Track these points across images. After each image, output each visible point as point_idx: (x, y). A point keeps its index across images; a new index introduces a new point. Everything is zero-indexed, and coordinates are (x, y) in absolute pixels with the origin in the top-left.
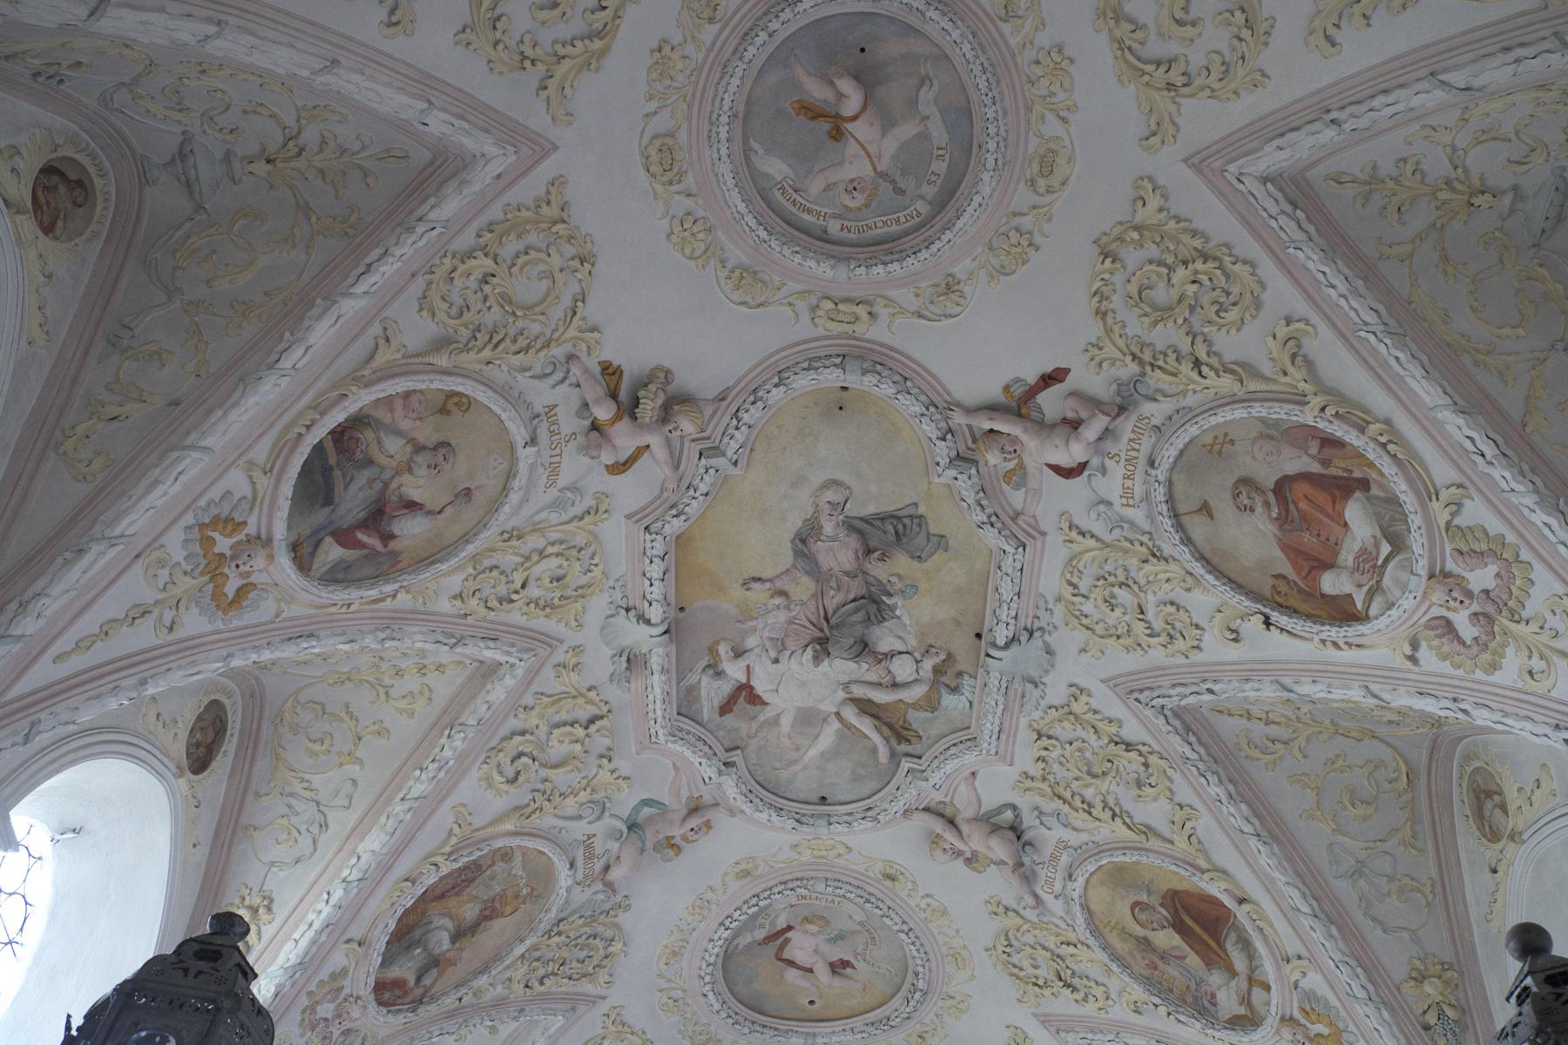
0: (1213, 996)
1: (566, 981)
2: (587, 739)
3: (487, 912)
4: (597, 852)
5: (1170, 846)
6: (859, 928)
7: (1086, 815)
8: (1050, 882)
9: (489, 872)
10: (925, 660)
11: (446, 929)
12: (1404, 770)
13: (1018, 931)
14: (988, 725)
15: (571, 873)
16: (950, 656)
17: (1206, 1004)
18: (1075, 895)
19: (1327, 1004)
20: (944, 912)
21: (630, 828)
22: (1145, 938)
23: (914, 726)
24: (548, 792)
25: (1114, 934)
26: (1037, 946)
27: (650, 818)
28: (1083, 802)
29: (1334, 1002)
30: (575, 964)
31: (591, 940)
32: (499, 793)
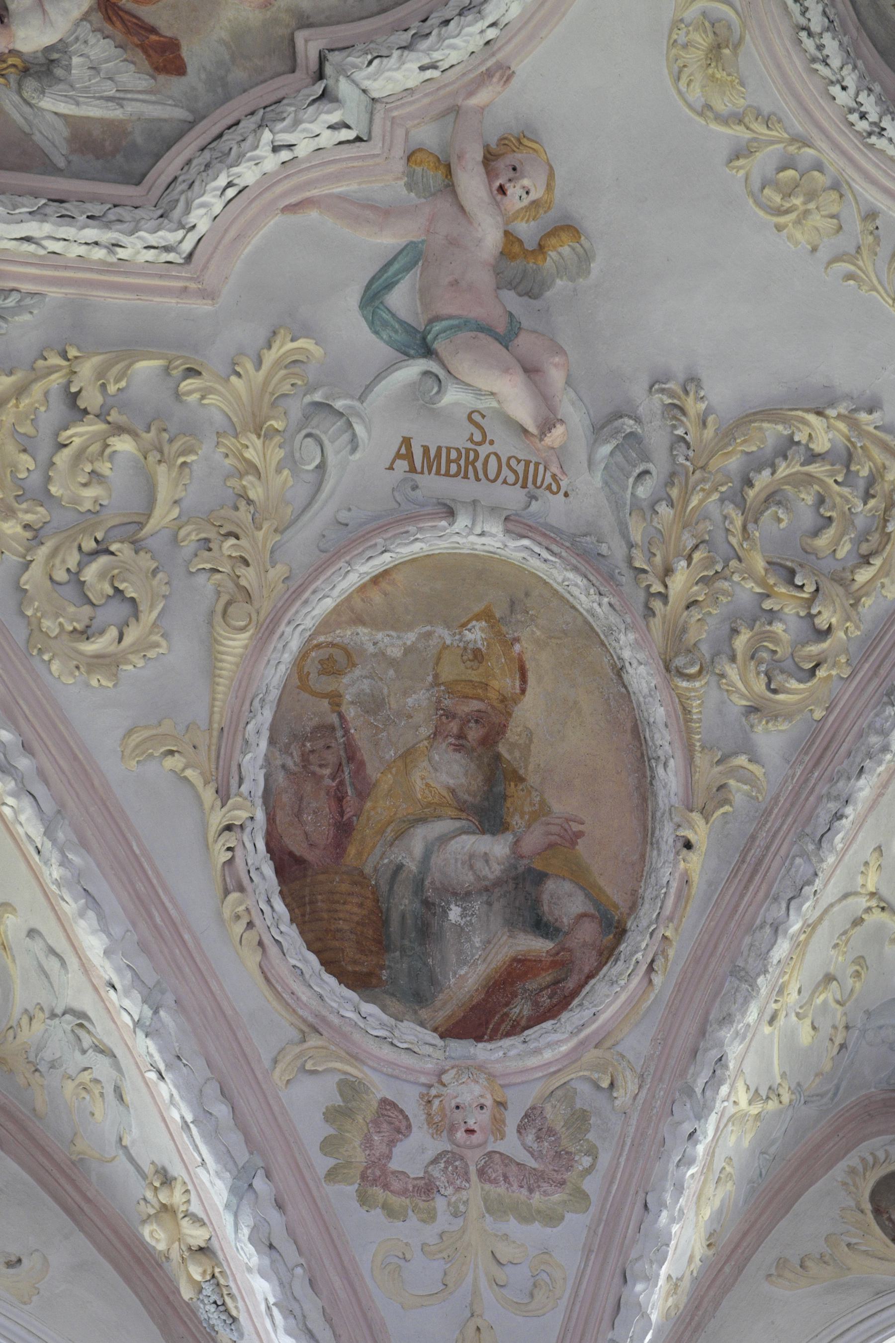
1: (863, 576)
2: (114, 416)
3: (474, 733)
4: (462, 443)
9: (351, 712)
11: (444, 839)
15: (462, 521)
21: (428, 352)
24: (211, 534)
27: (425, 293)
30: (823, 541)
31: (751, 493)
32: (143, 647)
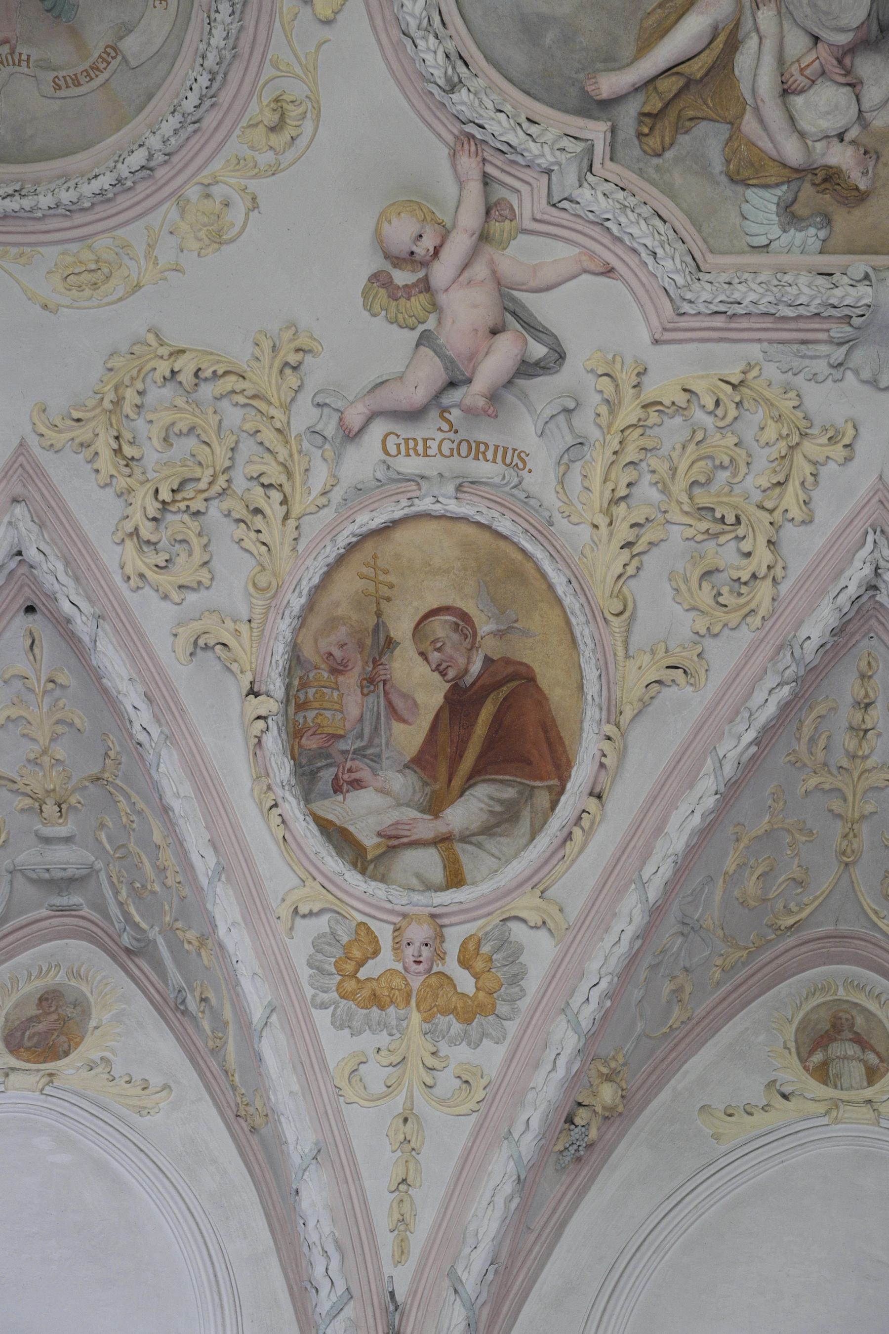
0: (357, 784)
5: (621, 653)
6: (96, 49)
7: (608, 495)
8: (409, 448)
10: (850, 151)
12: (804, 914)
13: (255, 397)
14: (752, 296)
16: (860, 197)
17: (327, 775)
18: (425, 505)
19: (516, 979)
20: (218, 239)
22: (390, 644)
23: (684, 140)
25: (360, 584)
26: (230, 441)
28: (629, 485)
29: (532, 984)
